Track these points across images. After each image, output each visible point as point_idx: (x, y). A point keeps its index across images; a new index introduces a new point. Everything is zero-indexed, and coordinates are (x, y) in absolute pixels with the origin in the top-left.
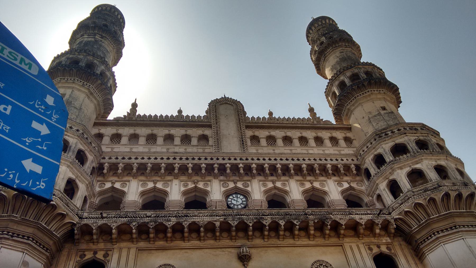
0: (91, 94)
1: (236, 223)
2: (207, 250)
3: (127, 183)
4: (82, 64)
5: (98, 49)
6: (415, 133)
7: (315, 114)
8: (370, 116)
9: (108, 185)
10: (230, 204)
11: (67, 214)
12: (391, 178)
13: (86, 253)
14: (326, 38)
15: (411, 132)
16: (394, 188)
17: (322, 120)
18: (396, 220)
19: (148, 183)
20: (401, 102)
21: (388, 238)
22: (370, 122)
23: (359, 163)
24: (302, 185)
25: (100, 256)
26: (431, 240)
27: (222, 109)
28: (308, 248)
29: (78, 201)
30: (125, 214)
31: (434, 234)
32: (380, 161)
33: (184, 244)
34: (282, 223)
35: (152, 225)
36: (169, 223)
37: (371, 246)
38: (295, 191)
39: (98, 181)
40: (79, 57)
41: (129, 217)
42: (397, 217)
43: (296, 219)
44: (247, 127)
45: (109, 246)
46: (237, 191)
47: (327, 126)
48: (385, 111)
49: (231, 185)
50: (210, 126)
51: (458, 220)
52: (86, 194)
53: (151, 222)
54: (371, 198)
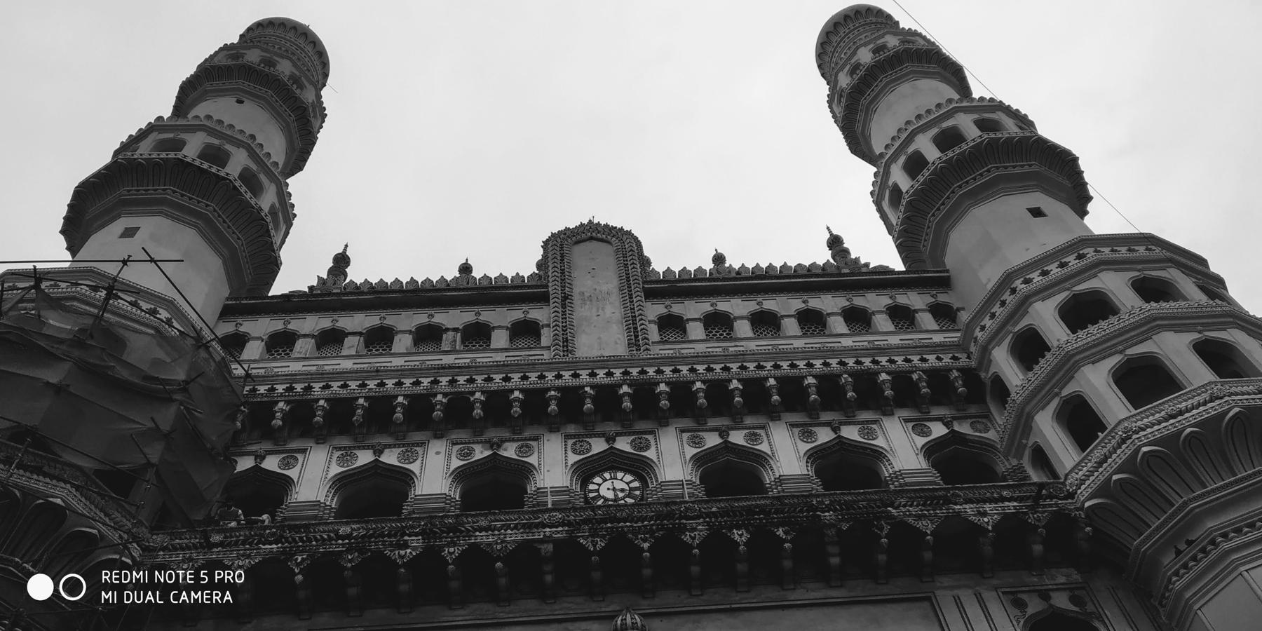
1: (601, 544)
3: (298, 455)
7: (846, 252)
10: (594, 498)
17: (867, 265)
19: (358, 453)
20: (1090, 199)
21: (1072, 571)
23: (973, 364)
24: (807, 435)
27: (581, 255)
28: (826, 610)
30: (273, 534)
32: (1030, 347)
34: (740, 536)
36: (402, 552)
37: (1020, 596)
41: (287, 541)
46: (612, 462)
47: (880, 279)
49: (598, 446)
50: (543, 299)
53: (349, 551)
54: (1014, 462)
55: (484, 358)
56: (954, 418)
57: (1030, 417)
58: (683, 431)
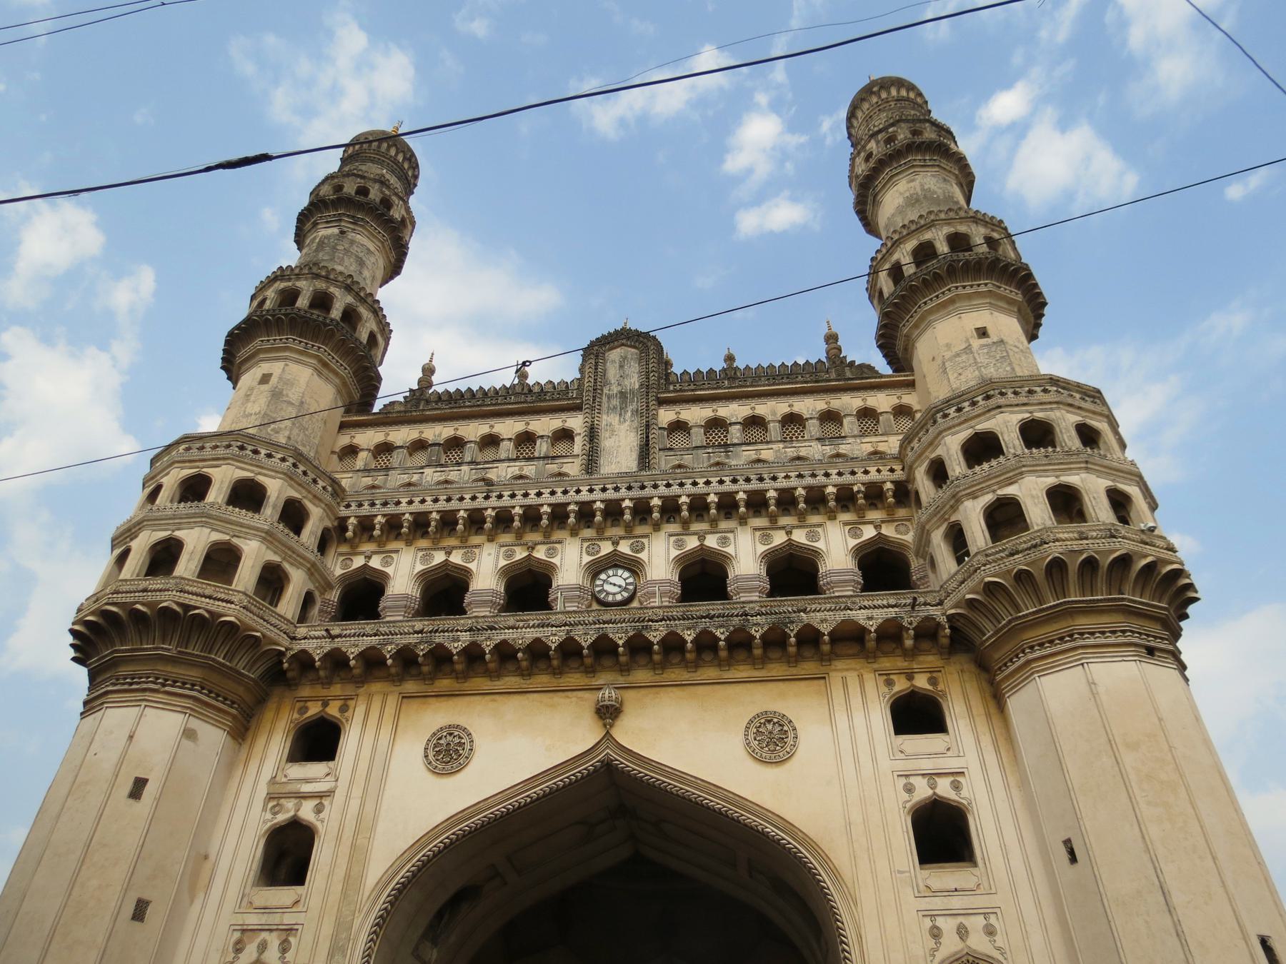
0: (325, 365)
1: (590, 641)
2: (536, 695)
6: (1024, 405)
8: (948, 355)
9: (358, 562)
11: (264, 636)
12: (953, 519)
13: (309, 704)
14: (878, 142)
18: (951, 618)
19: (434, 553)
20: (1045, 304)
22: (945, 371)
24: (766, 538)
25: (333, 710)
28: (748, 685)
29: (289, 605)
31: (1023, 652)
33: (489, 683)
34: (689, 636)
35: (422, 650)
42: (953, 611)
43: (721, 626)
44: (662, 402)
45: (349, 690)
46: (615, 562)
47: (862, 379)
48: (984, 341)
49: (606, 548)
50: (577, 408)
51: (1083, 622)
52: (311, 587)
54: (921, 561)
56: (883, 522)
57: (929, 534)
58: (671, 535)
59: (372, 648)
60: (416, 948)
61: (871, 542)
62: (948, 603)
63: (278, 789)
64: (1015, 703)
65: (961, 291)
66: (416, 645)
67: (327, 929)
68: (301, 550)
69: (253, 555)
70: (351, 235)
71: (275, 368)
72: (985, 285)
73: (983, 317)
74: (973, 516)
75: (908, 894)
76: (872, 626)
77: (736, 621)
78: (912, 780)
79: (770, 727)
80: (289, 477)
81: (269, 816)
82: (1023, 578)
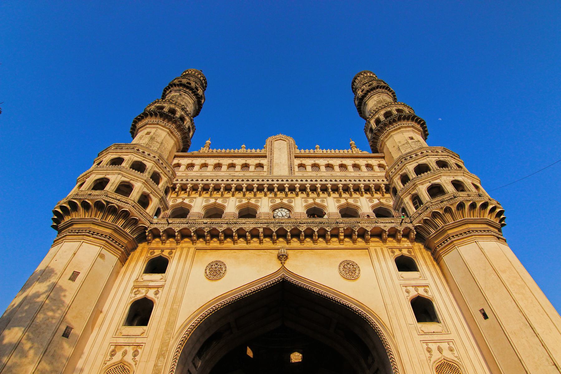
0: (172, 133)
1: (276, 230)
4: (166, 110)
5: (182, 100)
11: (140, 220)
12: (413, 193)
13: (155, 251)
15: (433, 154)
16: (416, 200)
18: (416, 228)
20: (428, 134)
21: (410, 243)
22: (399, 150)
23: (388, 183)
24: (338, 201)
25: (166, 253)
26: (447, 243)
32: (405, 179)
34: (316, 229)
35: (207, 230)
38: (332, 205)
39: (172, 198)
40: (164, 105)
44: (296, 157)
48: (412, 141)
49: (278, 201)
50: (265, 157)
55: (247, 174)
57: (402, 199)
59: (185, 229)
60: (194, 359)
61: (377, 205)
62: (414, 222)
63: (138, 284)
64: (446, 259)
65: (403, 125)
66: (204, 228)
67: (157, 345)
68: (158, 191)
69: (138, 188)
70: (183, 96)
71: (153, 131)
72: (411, 123)
73: (412, 134)
74: (423, 190)
75: (415, 334)
76: (387, 229)
77: (334, 226)
78: (408, 288)
79: (349, 266)
80: (156, 163)
81: (133, 295)
82: (448, 210)
